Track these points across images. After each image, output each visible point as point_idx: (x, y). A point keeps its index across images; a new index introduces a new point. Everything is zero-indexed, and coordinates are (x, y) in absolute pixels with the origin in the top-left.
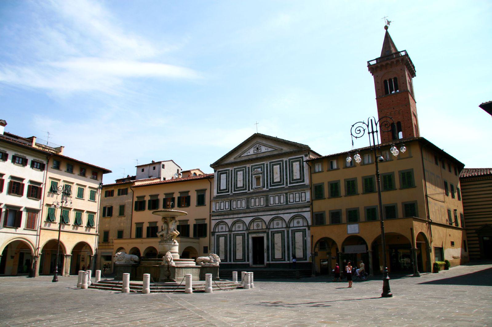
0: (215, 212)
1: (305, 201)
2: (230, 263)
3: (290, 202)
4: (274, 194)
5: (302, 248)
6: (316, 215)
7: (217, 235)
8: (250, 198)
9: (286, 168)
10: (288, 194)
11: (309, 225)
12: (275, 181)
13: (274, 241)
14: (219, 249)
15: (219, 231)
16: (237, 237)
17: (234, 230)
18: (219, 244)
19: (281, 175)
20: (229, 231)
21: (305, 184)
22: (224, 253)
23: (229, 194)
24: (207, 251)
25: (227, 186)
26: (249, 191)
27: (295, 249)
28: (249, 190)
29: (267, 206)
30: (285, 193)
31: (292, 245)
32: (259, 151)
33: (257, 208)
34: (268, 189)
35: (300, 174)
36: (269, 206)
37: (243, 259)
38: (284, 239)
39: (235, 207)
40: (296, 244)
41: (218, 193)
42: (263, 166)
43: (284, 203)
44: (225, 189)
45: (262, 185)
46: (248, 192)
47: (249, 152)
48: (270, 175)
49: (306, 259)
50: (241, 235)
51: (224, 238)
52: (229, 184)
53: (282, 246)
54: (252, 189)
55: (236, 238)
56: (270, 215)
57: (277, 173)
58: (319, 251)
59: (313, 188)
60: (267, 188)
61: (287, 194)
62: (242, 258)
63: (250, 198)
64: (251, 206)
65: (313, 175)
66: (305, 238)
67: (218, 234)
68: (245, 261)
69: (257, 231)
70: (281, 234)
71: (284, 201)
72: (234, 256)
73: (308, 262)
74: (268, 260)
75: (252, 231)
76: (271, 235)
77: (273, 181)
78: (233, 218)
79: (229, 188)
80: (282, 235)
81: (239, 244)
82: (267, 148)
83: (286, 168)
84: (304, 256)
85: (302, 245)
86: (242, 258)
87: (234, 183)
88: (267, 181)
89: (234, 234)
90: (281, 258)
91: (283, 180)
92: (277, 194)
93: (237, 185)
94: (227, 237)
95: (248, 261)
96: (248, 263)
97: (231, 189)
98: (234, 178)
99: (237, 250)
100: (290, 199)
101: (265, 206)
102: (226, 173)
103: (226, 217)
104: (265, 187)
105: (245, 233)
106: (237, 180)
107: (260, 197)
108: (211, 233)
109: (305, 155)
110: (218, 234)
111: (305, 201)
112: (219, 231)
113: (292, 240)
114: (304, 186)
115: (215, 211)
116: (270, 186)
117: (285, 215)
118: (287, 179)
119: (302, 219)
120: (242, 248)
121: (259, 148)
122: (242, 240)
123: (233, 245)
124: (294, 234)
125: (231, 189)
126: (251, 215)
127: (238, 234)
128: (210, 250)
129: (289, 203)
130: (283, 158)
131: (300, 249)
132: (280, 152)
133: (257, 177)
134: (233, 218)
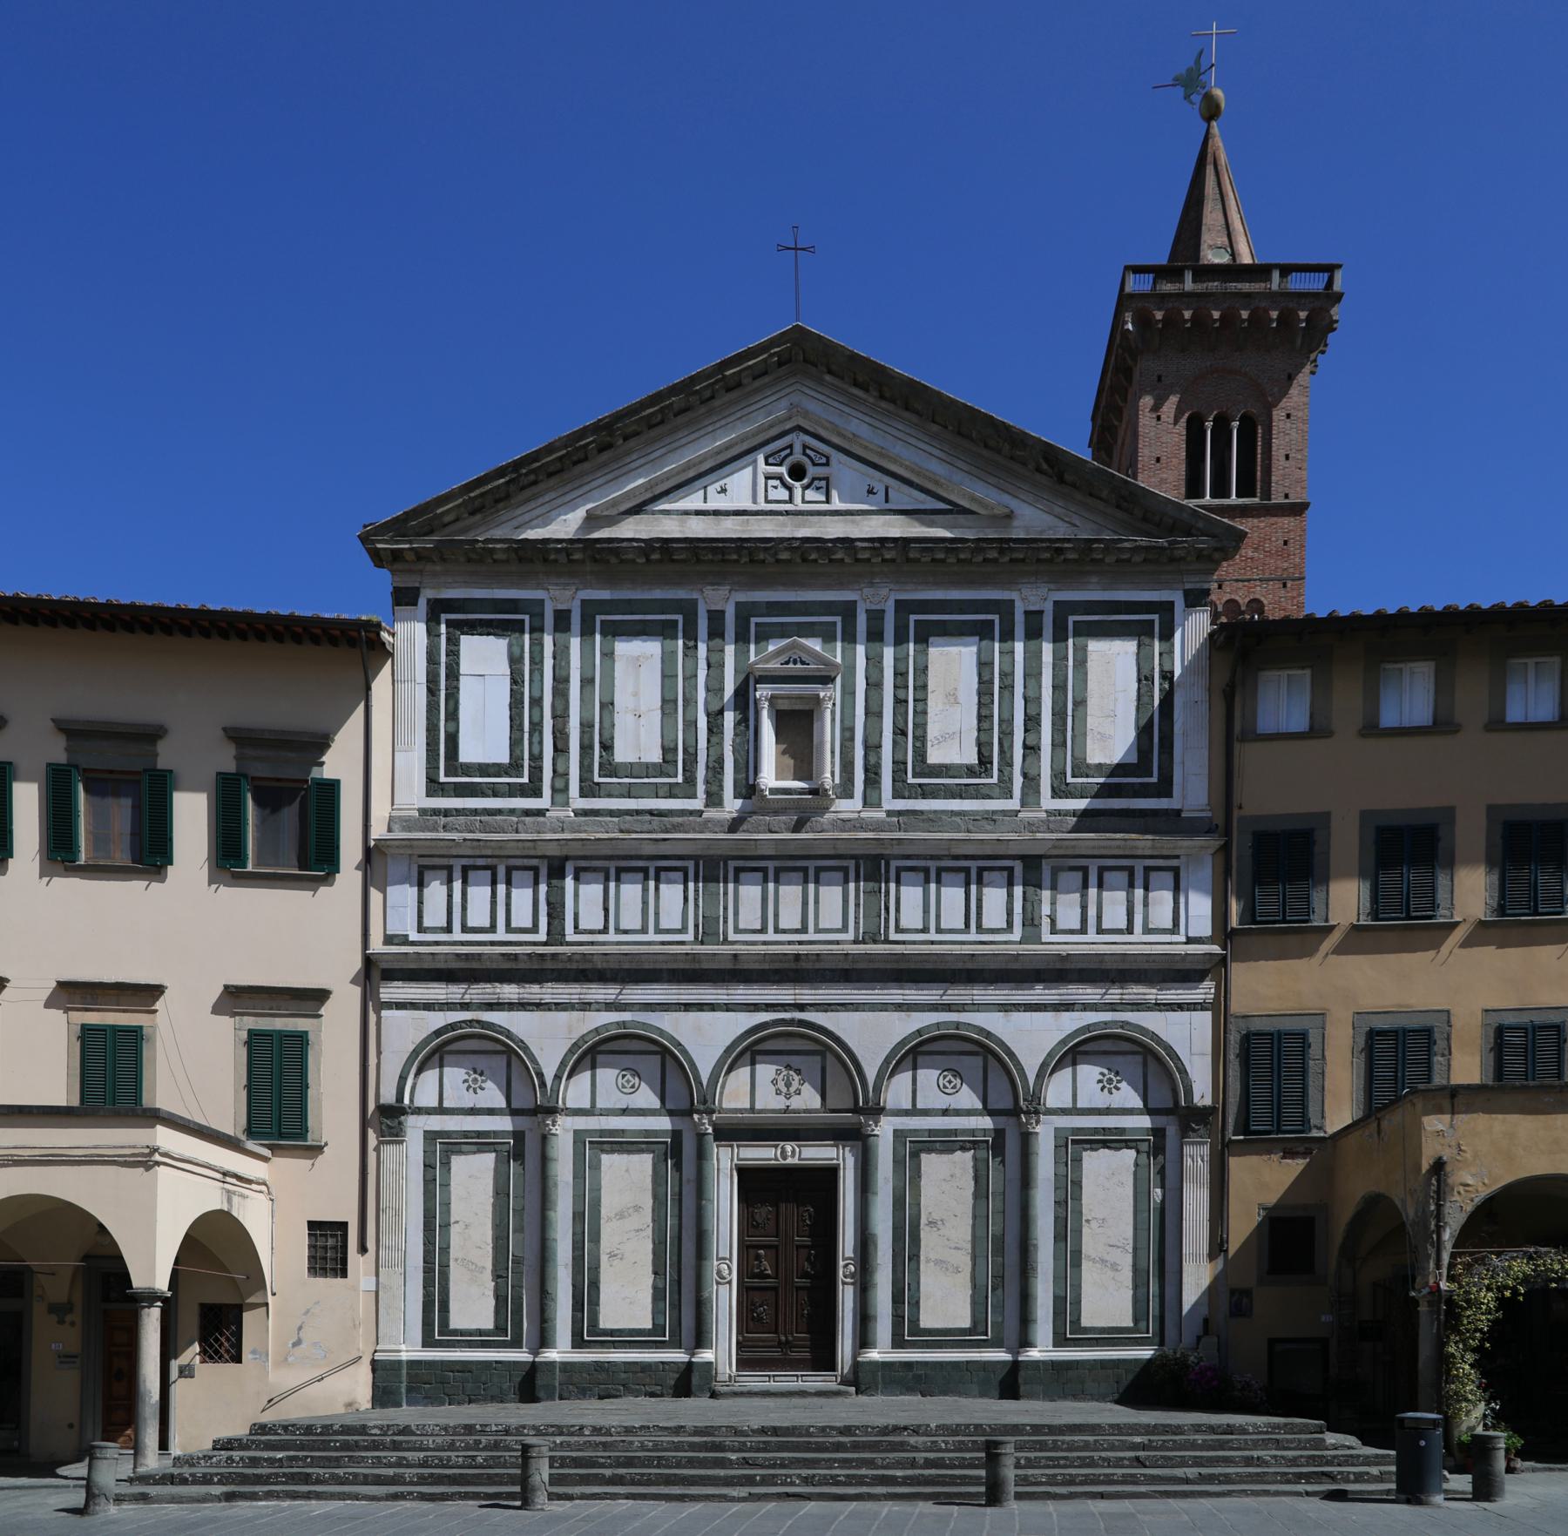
1: (1175, 929)
3: (1054, 931)
4: (932, 857)
8: (732, 864)
11: (1197, 1100)
12: (934, 757)
19: (983, 718)
21: (1178, 812)
23: (540, 813)
25: (515, 743)
33: (803, 949)
34: (880, 815)
39: (592, 917)
42: (838, 619)
43: (1010, 926)
44: (498, 765)
45: (833, 773)
46: (711, 814)
48: (900, 702)
52: (536, 727)
57: (952, 698)
59: (1241, 846)
60: (865, 804)
61: (1039, 868)
63: (726, 859)
64: (737, 930)
65: (1250, 756)
71: (1010, 913)
77: (921, 754)
79: (536, 759)
87: (586, 726)
88: (872, 748)
91: (1007, 762)
92: (956, 858)
93: (607, 747)
97: (560, 775)
103: (510, 991)
104: (848, 794)
106: (608, 705)
107: (811, 864)
111: (1175, 929)
114: (1171, 822)
116: (897, 795)
117: (1017, 1017)
118: (1031, 749)
119: (1139, 1058)
125: (560, 775)
126: (742, 993)
129: (1046, 936)
130: (1010, 584)
133: (784, 705)
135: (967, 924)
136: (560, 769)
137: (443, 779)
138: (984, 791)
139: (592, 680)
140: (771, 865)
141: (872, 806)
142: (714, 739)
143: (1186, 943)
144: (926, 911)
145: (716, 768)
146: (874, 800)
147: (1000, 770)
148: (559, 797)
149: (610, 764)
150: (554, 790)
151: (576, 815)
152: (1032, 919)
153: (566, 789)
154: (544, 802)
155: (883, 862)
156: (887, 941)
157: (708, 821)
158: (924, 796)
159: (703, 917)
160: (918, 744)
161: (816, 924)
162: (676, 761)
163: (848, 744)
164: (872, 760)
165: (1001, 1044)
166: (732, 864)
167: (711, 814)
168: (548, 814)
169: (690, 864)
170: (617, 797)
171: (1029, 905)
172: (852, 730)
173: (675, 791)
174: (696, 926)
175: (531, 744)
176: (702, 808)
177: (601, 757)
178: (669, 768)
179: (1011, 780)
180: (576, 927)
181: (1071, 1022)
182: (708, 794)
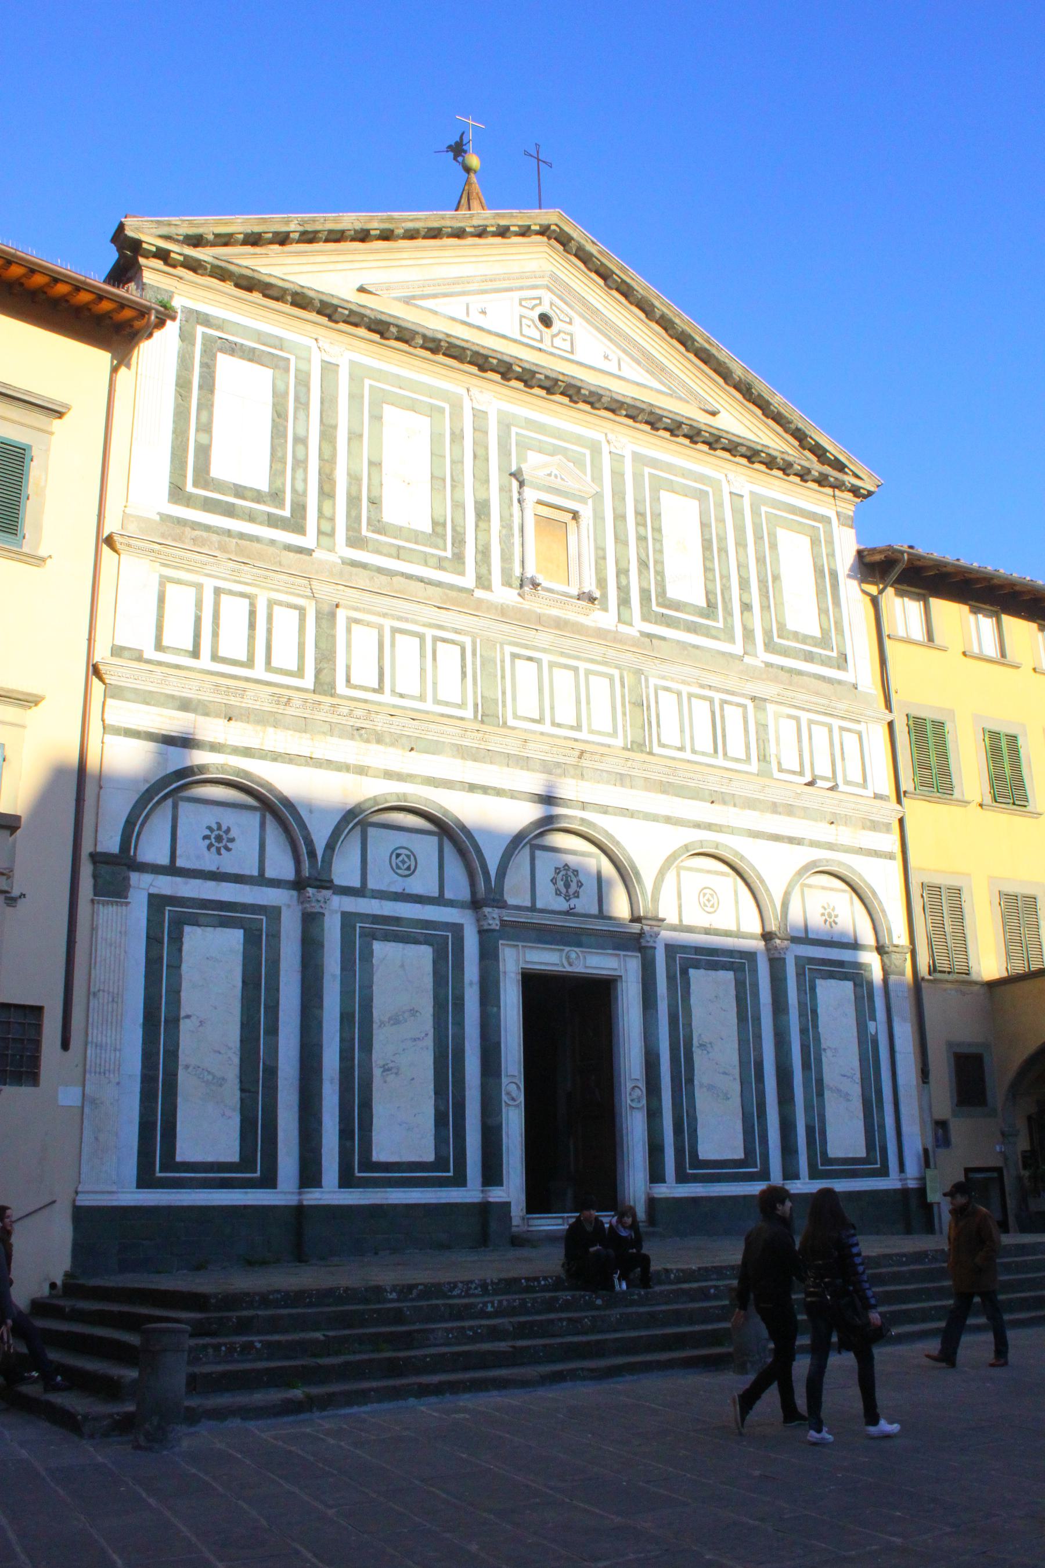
0: (149, 662)
2: (314, 1197)
3: (781, 770)
4: (683, 682)
5: (855, 1090)
6: (933, 890)
7: (157, 903)
9: (741, 544)
10: (771, 708)
13: (689, 1025)
14: (172, 1054)
15: (180, 863)
16: (377, 946)
17: (356, 883)
18: (175, 992)
20: (299, 885)
22: (232, 1093)
23: (309, 552)
24: (35, 1060)
26: (488, 588)
27: (820, 1094)
28: (483, 581)
29: (638, 746)
30: (753, 699)
31: (806, 1066)
32: (557, 341)
35: (823, 611)
36: (651, 753)
37: (440, 1163)
38: (757, 1019)
40: (824, 1059)
41: (177, 493)
47: (484, 312)
49: (884, 1172)
50: (426, 941)
51: (235, 937)
53: (743, 1064)
54: (507, 583)
55: (367, 956)
56: (668, 820)
58: (955, 1114)
60: (620, 620)
62: (430, 1157)
66: (871, 1026)
67: (165, 885)
68: (460, 1180)
69: (571, 923)
70: (730, 975)
72: (345, 1133)
73: (898, 1185)
74: (656, 1175)
75: (523, 918)
76: (671, 978)
78: (361, 770)
80: (740, 985)
81: (395, 1020)
82: (615, 353)
83: (741, 544)
84: (870, 1145)
85: (858, 1075)
86: (430, 1157)
87: (354, 479)
89: (348, 919)
90: (740, 1155)
94: (275, 936)
95: (492, 1175)
96: (496, 1195)
98: (354, 437)
99: (377, 1072)
100: (778, 744)
101: (625, 749)
102: (279, 365)
105: (457, 930)
108: (86, 870)
109: (838, 514)
110: (165, 885)
111: (864, 784)
112: (180, 863)
113: (804, 1031)
115: (150, 653)
120: (428, 1059)
121: (557, 325)
122: (428, 982)
123: (346, 1018)
124: (813, 988)
127: (397, 920)
128: (65, 1045)
131: (847, 1097)
132: (703, 419)
134: (361, 770)
135: (716, 751)
136: (327, 512)
137: (190, 488)
138: (714, 632)
139: (361, 436)
140: (545, 658)
141: (625, 623)
142: (482, 525)
143: (875, 798)
144: (682, 731)
145: (484, 554)
146: (625, 616)
147: (725, 619)
148: (325, 540)
149: (379, 521)
150: (320, 532)
151: (343, 563)
152: (765, 756)
153: (332, 534)
154: (308, 540)
155: (643, 677)
156: (651, 753)
157: (480, 601)
158: (668, 625)
159: (482, 697)
160: (659, 578)
161: (589, 725)
162: (445, 535)
163: (601, 562)
164: (624, 582)
165: (754, 869)
166: (509, 649)
167: (479, 593)
168: (314, 554)
169: (467, 641)
170: (385, 555)
171: (761, 742)
172: (604, 550)
173: (445, 564)
174: (476, 705)
175: (293, 479)
176: (476, 590)
177: (369, 511)
178: (440, 542)
179: (733, 627)
180: (348, 680)
181: (807, 855)
182: (479, 578)
